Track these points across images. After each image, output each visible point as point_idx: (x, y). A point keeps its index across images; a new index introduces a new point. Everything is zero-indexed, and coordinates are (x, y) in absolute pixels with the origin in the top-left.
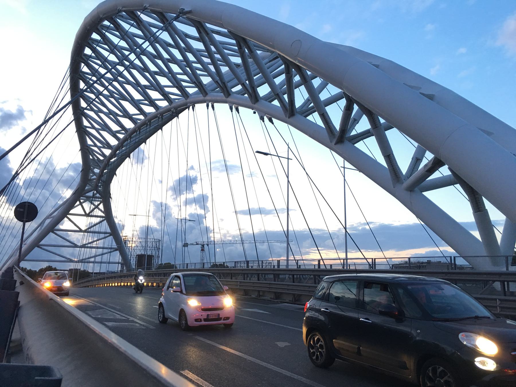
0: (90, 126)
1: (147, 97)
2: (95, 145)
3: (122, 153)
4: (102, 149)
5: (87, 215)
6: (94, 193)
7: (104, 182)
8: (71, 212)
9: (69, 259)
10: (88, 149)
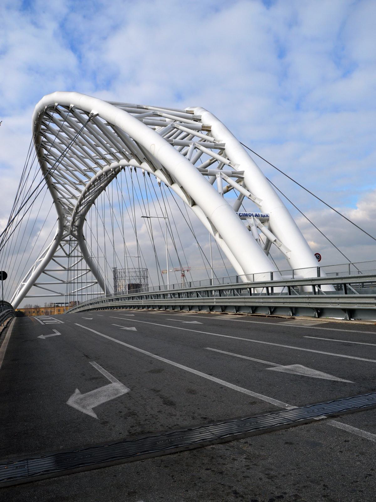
0: (57, 182)
1: (99, 153)
2: (64, 197)
3: (87, 201)
7: (77, 227)
8: (55, 254)
9: (60, 293)
10: (59, 201)
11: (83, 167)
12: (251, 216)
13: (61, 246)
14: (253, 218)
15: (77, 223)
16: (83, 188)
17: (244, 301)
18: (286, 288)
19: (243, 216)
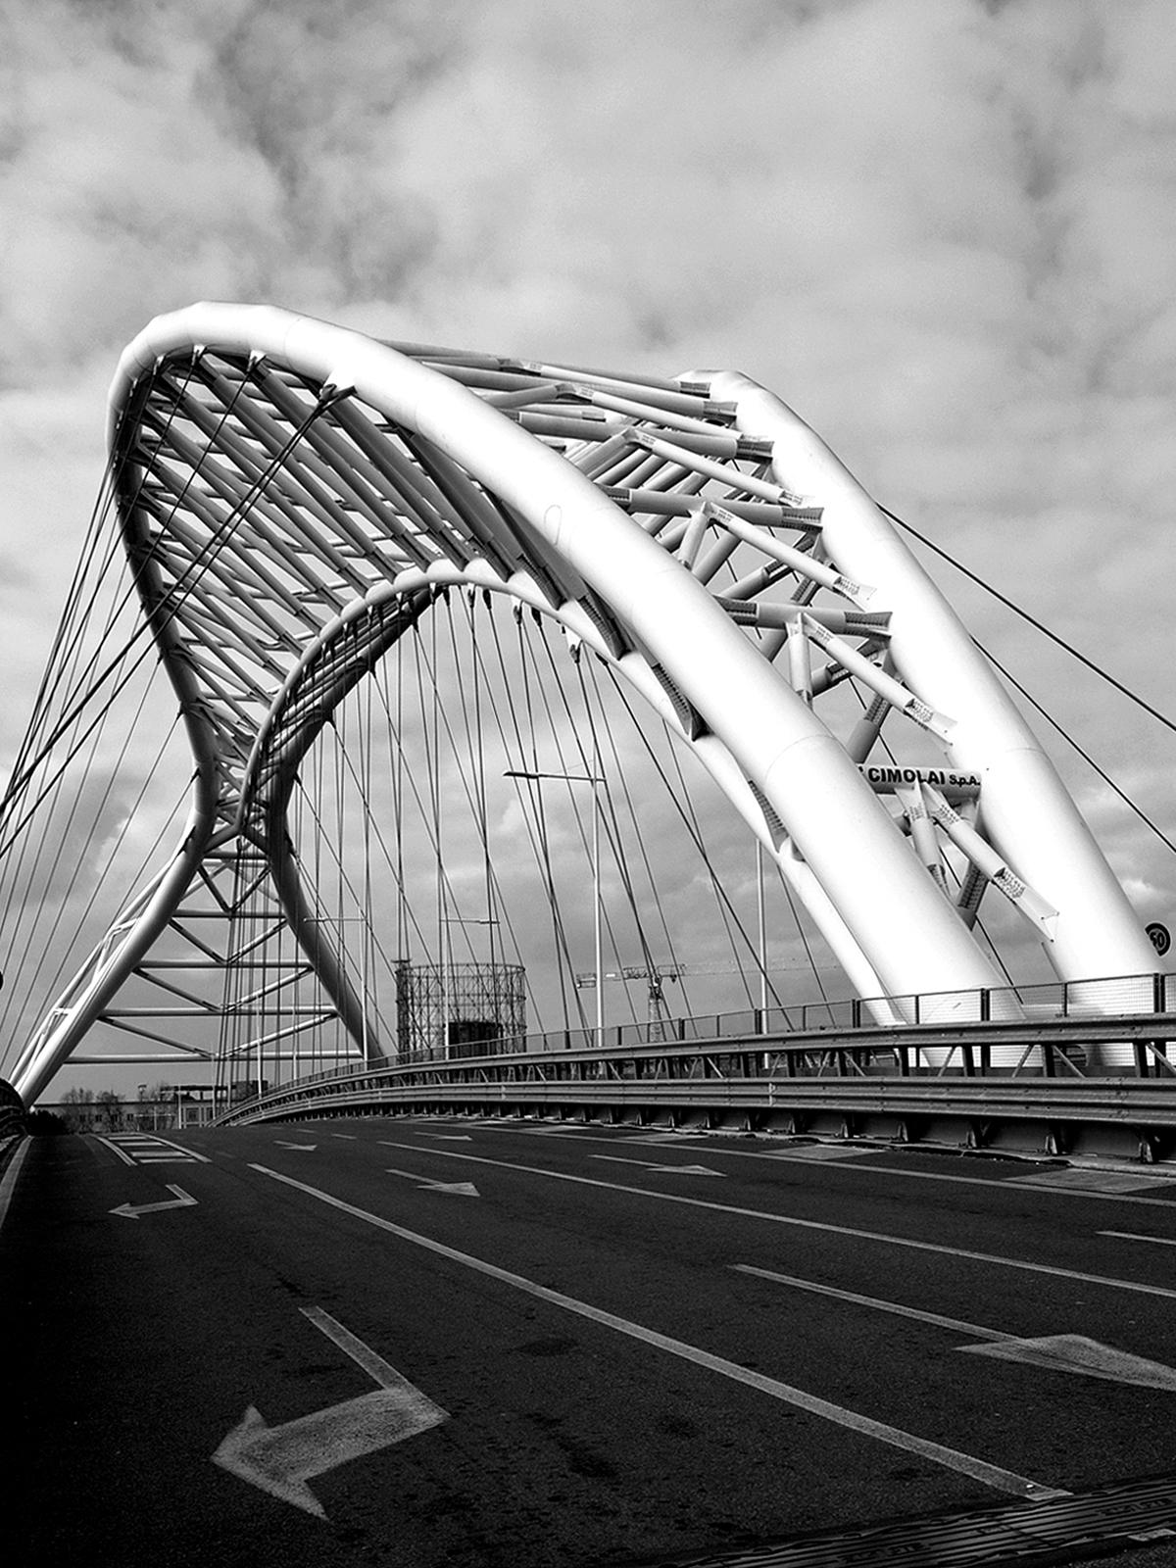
2: (221, 695)
4: (243, 705)
5: (230, 913)
6: (238, 841)
7: (265, 804)
9: (196, 1050)
10: (202, 710)
11: (293, 586)
12: (913, 780)
13: (204, 875)
14: (922, 788)
15: (264, 793)
16: (291, 663)
17: (880, 1095)
18: (959, 1050)
19: (884, 779)
